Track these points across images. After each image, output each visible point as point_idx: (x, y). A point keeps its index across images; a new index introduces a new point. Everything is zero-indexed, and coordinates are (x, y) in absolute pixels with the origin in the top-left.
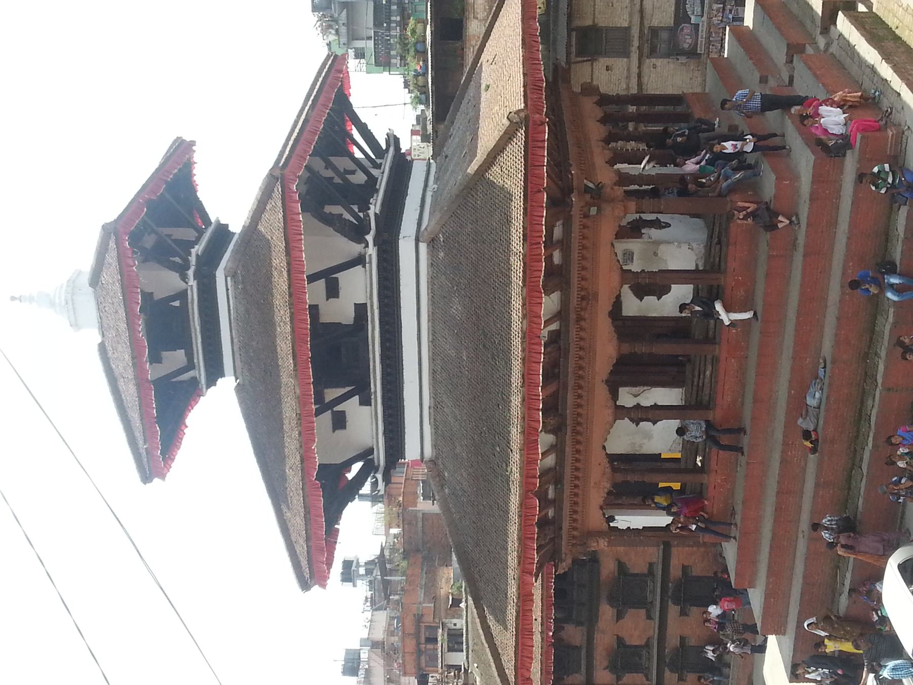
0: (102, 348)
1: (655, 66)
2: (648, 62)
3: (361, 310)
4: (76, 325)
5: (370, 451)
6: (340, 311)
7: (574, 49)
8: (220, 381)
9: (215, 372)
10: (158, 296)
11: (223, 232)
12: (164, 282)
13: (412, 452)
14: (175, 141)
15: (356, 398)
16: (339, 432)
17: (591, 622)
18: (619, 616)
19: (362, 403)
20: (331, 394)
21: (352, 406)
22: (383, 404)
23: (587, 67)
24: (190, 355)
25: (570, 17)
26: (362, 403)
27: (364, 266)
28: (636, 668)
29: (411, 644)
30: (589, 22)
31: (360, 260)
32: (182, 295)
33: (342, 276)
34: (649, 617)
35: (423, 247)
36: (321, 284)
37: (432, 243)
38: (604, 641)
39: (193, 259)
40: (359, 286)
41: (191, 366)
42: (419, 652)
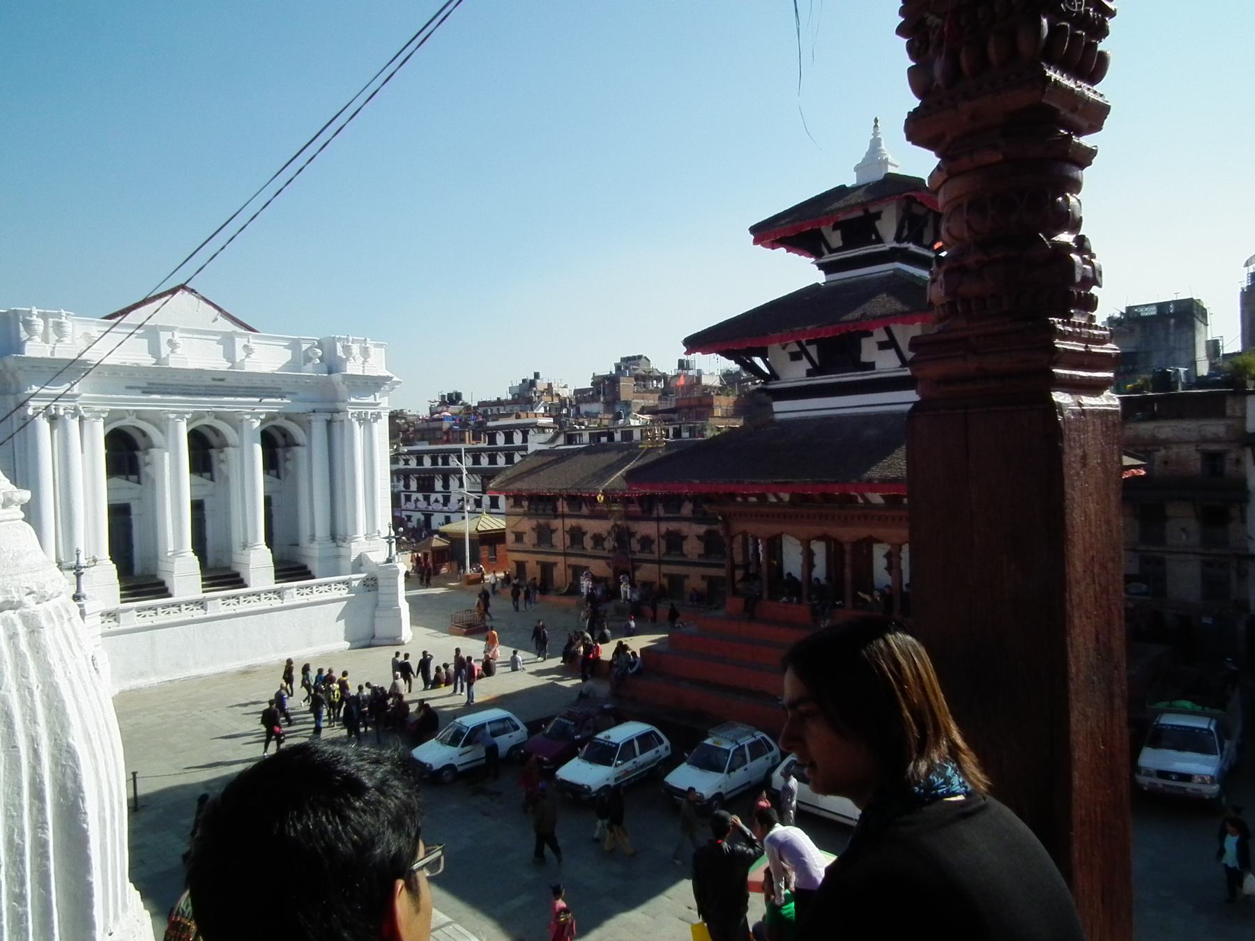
3: (871, 366)
4: (857, 169)
5: (777, 378)
8: (822, 272)
9: (827, 268)
10: (877, 223)
12: (888, 227)
13: (778, 406)
15: (810, 367)
17: (696, 519)
18: (699, 537)
20: (813, 350)
21: (805, 365)
28: (669, 547)
29: (694, 402)
32: (880, 240)
33: (892, 352)
34: (700, 556)
36: (885, 338)
38: (686, 528)
39: (905, 245)
40: (887, 364)
41: (832, 251)
42: (690, 408)
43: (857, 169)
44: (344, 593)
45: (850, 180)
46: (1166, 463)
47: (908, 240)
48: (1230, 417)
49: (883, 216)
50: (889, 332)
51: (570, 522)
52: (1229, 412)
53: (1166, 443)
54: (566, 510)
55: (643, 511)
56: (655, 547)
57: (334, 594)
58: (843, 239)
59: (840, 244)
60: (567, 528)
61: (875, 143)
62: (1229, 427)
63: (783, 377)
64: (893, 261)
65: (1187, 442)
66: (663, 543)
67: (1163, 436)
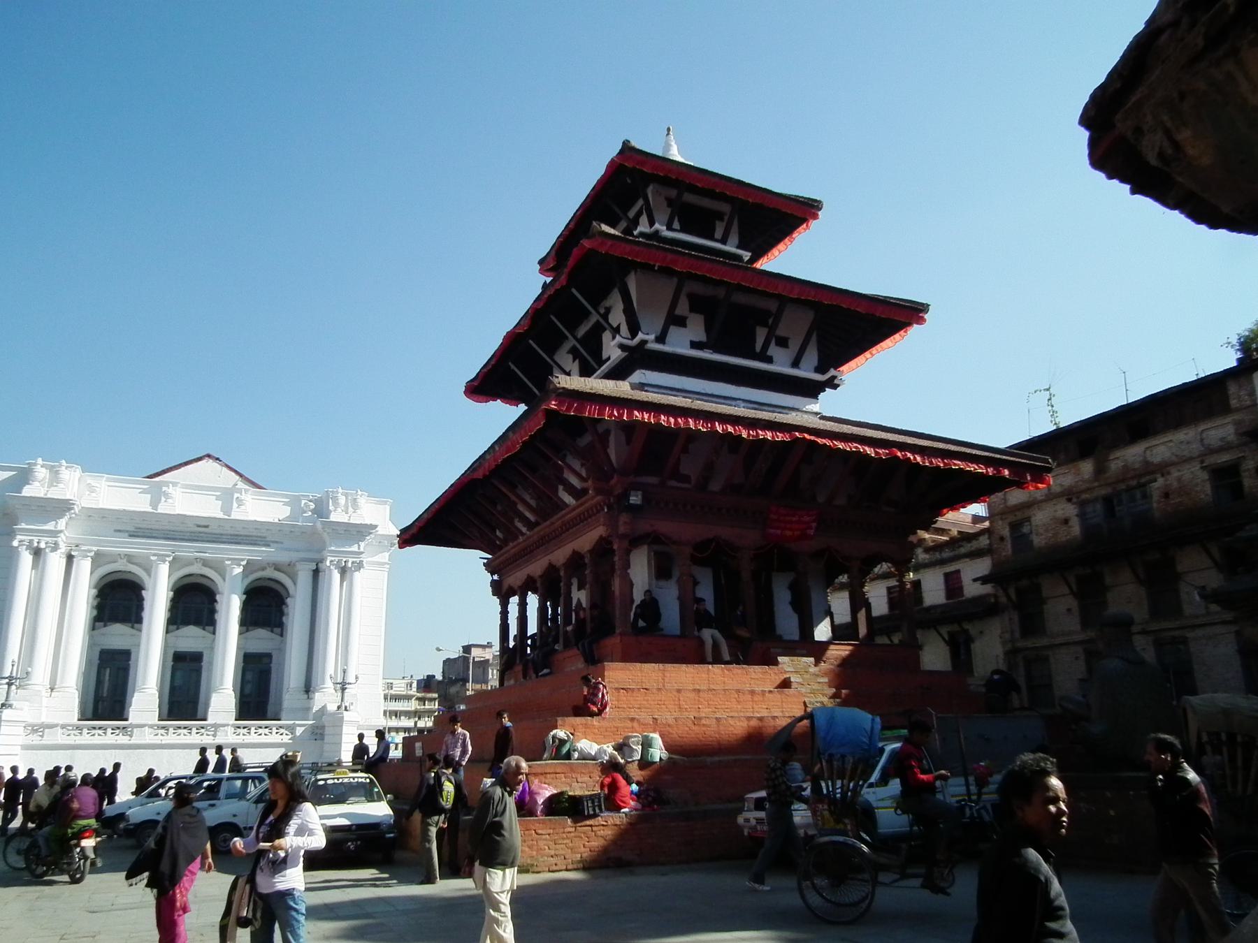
30: (1108, 580)
44: (286, 739)
46: (1166, 495)
48: (1237, 410)
52: (1234, 403)
53: (1163, 468)
57: (274, 738)
62: (1237, 424)
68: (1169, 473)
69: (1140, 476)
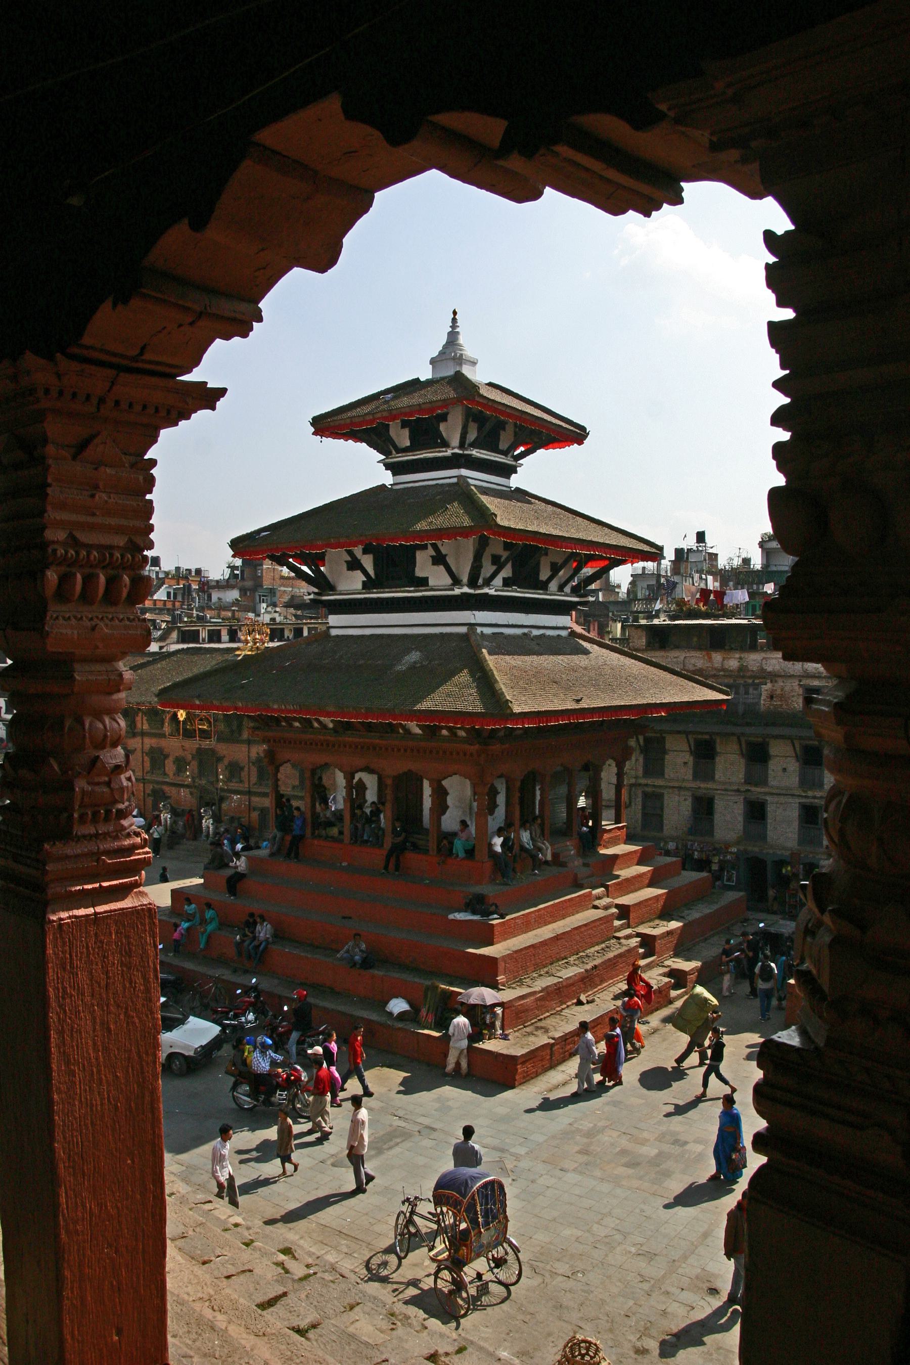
0: (417, 381)
1: (685, 800)
2: (689, 793)
3: (423, 582)
6: (423, 566)
7: (700, 736)
8: (389, 472)
9: (396, 469)
10: (442, 427)
11: (508, 471)
13: (333, 620)
14: (583, 429)
16: (345, 566)
19: (363, 582)
20: (368, 562)
22: (365, 599)
23: (686, 748)
24: (406, 450)
25: (717, 734)
26: (363, 582)
27: (453, 585)
30: (719, 748)
31: (456, 582)
32: (445, 444)
33: (442, 567)
34: (294, 787)
35: (464, 630)
37: (465, 637)
40: (439, 580)
43: (433, 362)
45: (426, 373)
46: (772, 697)
47: (473, 445)
49: (449, 417)
50: (435, 547)
51: (149, 742)
53: (773, 676)
54: (146, 727)
55: (232, 732)
56: (244, 774)
58: (410, 439)
59: (408, 444)
60: (147, 747)
61: (453, 336)
63: (341, 587)
64: (459, 467)
65: (792, 676)
66: (254, 770)
67: (769, 669)
68: (776, 681)
69: (754, 677)
